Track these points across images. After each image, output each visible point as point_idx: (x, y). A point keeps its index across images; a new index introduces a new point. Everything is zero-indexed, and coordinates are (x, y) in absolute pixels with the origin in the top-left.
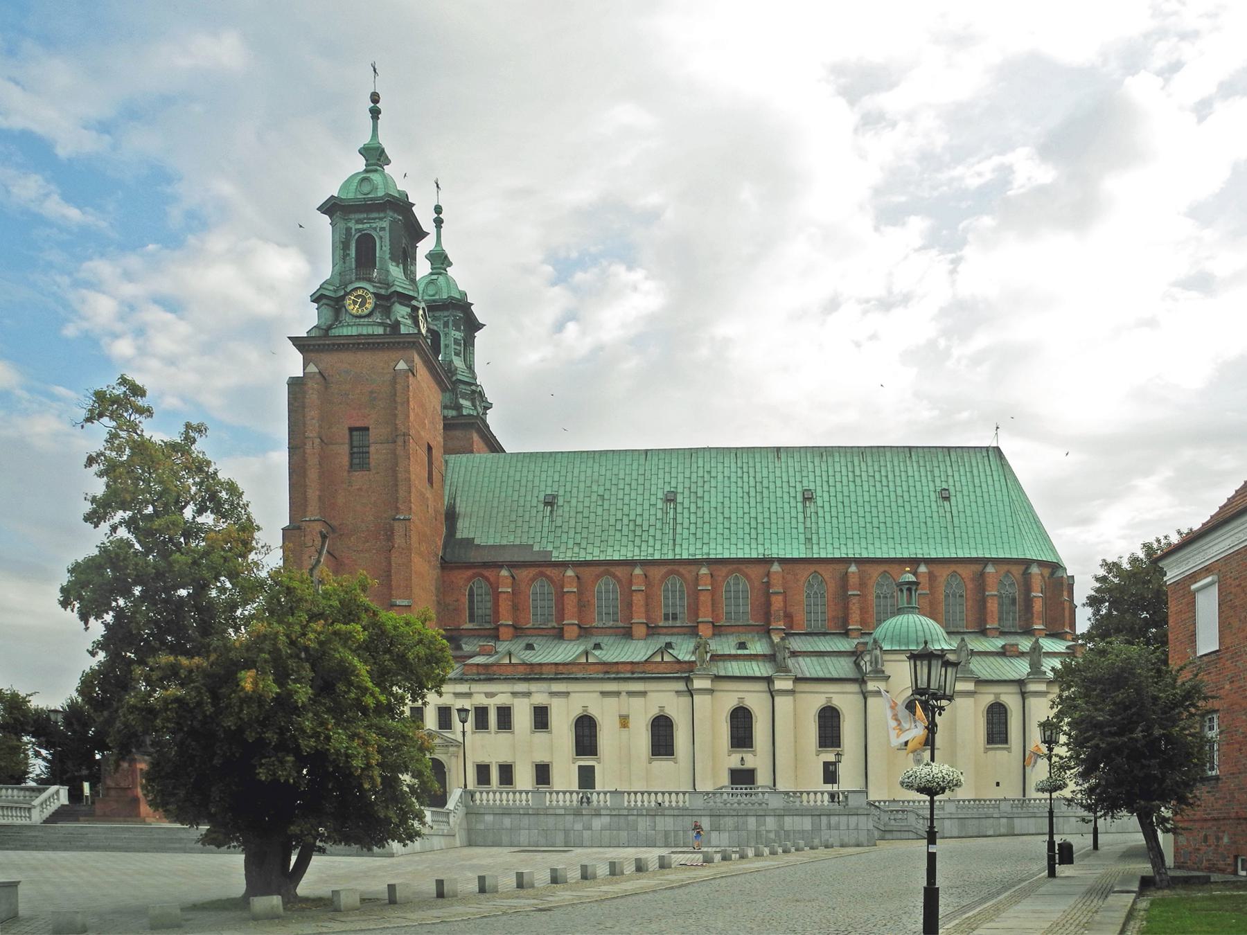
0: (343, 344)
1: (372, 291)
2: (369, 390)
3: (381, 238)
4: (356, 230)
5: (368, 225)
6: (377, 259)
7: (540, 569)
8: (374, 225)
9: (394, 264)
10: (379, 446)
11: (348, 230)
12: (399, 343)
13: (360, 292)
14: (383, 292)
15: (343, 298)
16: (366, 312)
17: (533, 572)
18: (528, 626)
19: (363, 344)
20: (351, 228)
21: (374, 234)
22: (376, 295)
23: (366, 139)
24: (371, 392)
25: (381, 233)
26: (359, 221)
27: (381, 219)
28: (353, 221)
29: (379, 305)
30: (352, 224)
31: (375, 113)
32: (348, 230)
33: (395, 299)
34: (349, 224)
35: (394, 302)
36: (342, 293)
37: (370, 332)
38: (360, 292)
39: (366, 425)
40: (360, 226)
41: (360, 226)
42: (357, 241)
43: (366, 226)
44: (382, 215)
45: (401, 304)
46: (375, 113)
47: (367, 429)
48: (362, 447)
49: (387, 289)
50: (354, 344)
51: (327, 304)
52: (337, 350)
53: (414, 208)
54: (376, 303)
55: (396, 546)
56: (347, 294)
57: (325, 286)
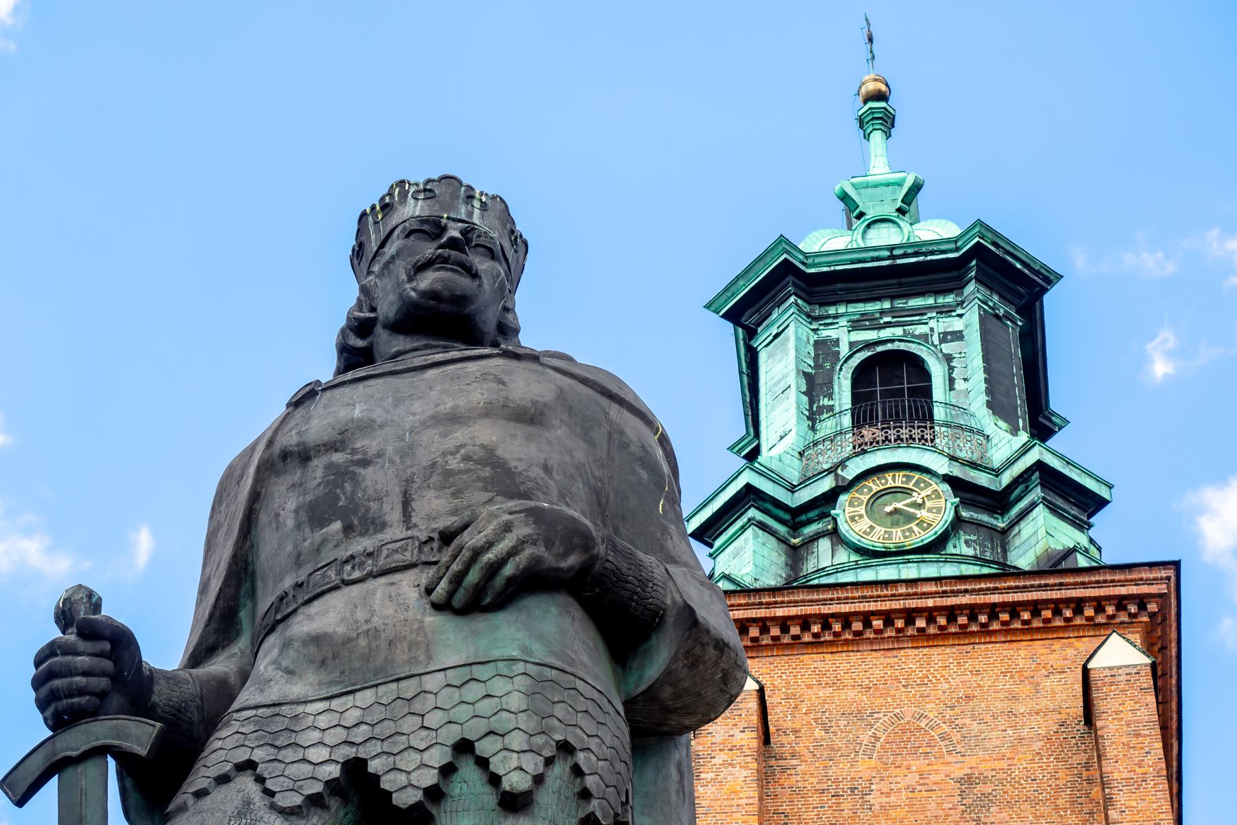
2: (960, 774)
3: (949, 358)
4: (852, 344)
5: (899, 331)
8: (920, 330)
11: (825, 349)
12: (1078, 605)
13: (895, 480)
14: (983, 479)
19: (930, 615)
24: (968, 781)
25: (947, 348)
26: (856, 325)
27: (945, 311)
28: (843, 322)
29: (971, 523)
30: (842, 334)
32: (825, 349)
36: (827, 484)
42: (861, 376)
43: (886, 333)
44: (950, 299)
49: (997, 472)
51: (763, 526)
52: (817, 644)
53: (1051, 300)
56: (842, 488)
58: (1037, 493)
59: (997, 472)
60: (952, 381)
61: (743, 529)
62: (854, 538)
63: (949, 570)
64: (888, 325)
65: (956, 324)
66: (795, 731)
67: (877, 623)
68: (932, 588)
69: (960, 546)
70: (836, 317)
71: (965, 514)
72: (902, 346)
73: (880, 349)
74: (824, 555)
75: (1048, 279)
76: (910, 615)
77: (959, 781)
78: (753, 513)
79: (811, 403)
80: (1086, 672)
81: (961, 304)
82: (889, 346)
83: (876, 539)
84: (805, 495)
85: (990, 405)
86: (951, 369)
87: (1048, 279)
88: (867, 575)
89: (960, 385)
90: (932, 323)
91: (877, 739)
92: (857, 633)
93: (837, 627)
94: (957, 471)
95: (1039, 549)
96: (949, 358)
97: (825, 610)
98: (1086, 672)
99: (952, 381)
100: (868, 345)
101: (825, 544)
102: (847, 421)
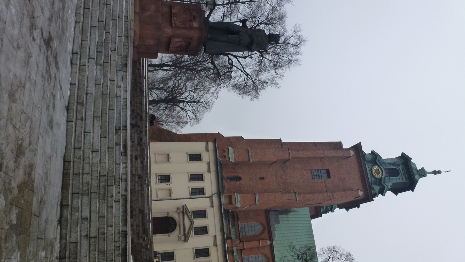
0: (362, 166)
1: (383, 177)
5: (402, 173)
6: (392, 177)
7: (271, 260)
8: (403, 175)
9: (391, 185)
10: (324, 183)
13: (381, 172)
14: (383, 181)
15: (377, 165)
16: (374, 174)
17: (269, 255)
18: (243, 255)
20: (400, 166)
21: (400, 175)
22: (381, 178)
23: (427, 170)
24: (345, 179)
26: (402, 169)
27: (406, 178)
28: (402, 167)
29: (377, 180)
31: (435, 172)
32: (398, 165)
33: (382, 187)
34: (401, 166)
35: (379, 186)
36: (379, 164)
37: (369, 177)
38: (381, 172)
39: (331, 176)
40: (401, 170)
41: (401, 170)
43: (402, 172)
44: (407, 179)
45: (380, 189)
46: (435, 172)
47: (329, 177)
48: (321, 175)
49: (384, 183)
50: (363, 170)
52: (359, 163)
53: (410, 191)
54: (378, 178)
55: (284, 195)
56: (379, 166)
57: (380, 157)
58: (382, 187)
59: (384, 183)
60: (396, 179)
61: (372, 156)
62: (373, 167)
63: (369, 177)
64: (403, 172)
65: (404, 180)
66: (348, 161)
67: (362, 169)
68: (367, 174)
69: (373, 179)
70: (403, 166)
71: (378, 179)
72: (400, 173)
73: (399, 171)
74: (370, 165)
75: (413, 191)
76: (363, 172)
77: (345, 178)
78: (374, 157)
79: (391, 164)
80: (358, 190)
81: (407, 180)
82: (400, 172)
83: (373, 170)
84: (378, 162)
85: (393, 183)
86: (398, 179)
87: (413, 191)
88: (367, 168)
89: (396, 180)
90: (404, 177)
91: (348, 169)
92: (360, 167)
93: (361, 165)
94: (383, 178)
95: (375, 187)
96: (399, 179)
97: (362, 163)
98: (358, 190)
99: (396, 179)
100: (400, 170)
101: (372, 165)
102: (389, 168)
